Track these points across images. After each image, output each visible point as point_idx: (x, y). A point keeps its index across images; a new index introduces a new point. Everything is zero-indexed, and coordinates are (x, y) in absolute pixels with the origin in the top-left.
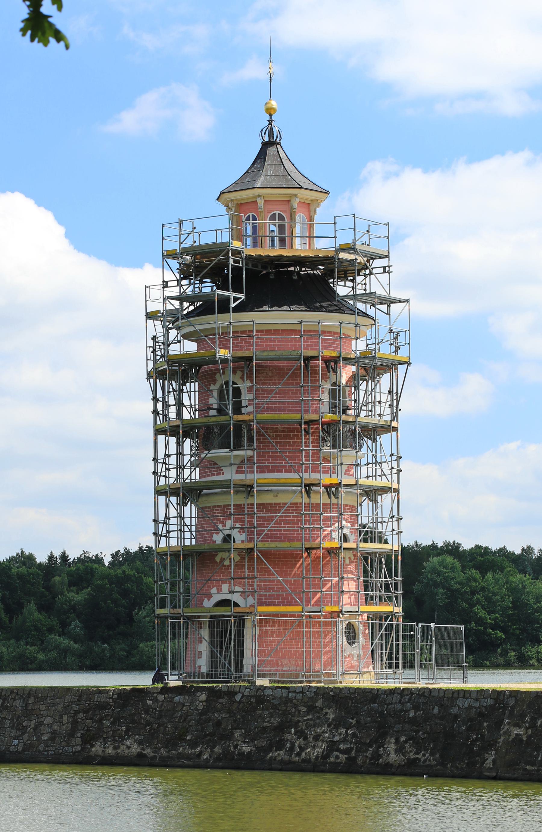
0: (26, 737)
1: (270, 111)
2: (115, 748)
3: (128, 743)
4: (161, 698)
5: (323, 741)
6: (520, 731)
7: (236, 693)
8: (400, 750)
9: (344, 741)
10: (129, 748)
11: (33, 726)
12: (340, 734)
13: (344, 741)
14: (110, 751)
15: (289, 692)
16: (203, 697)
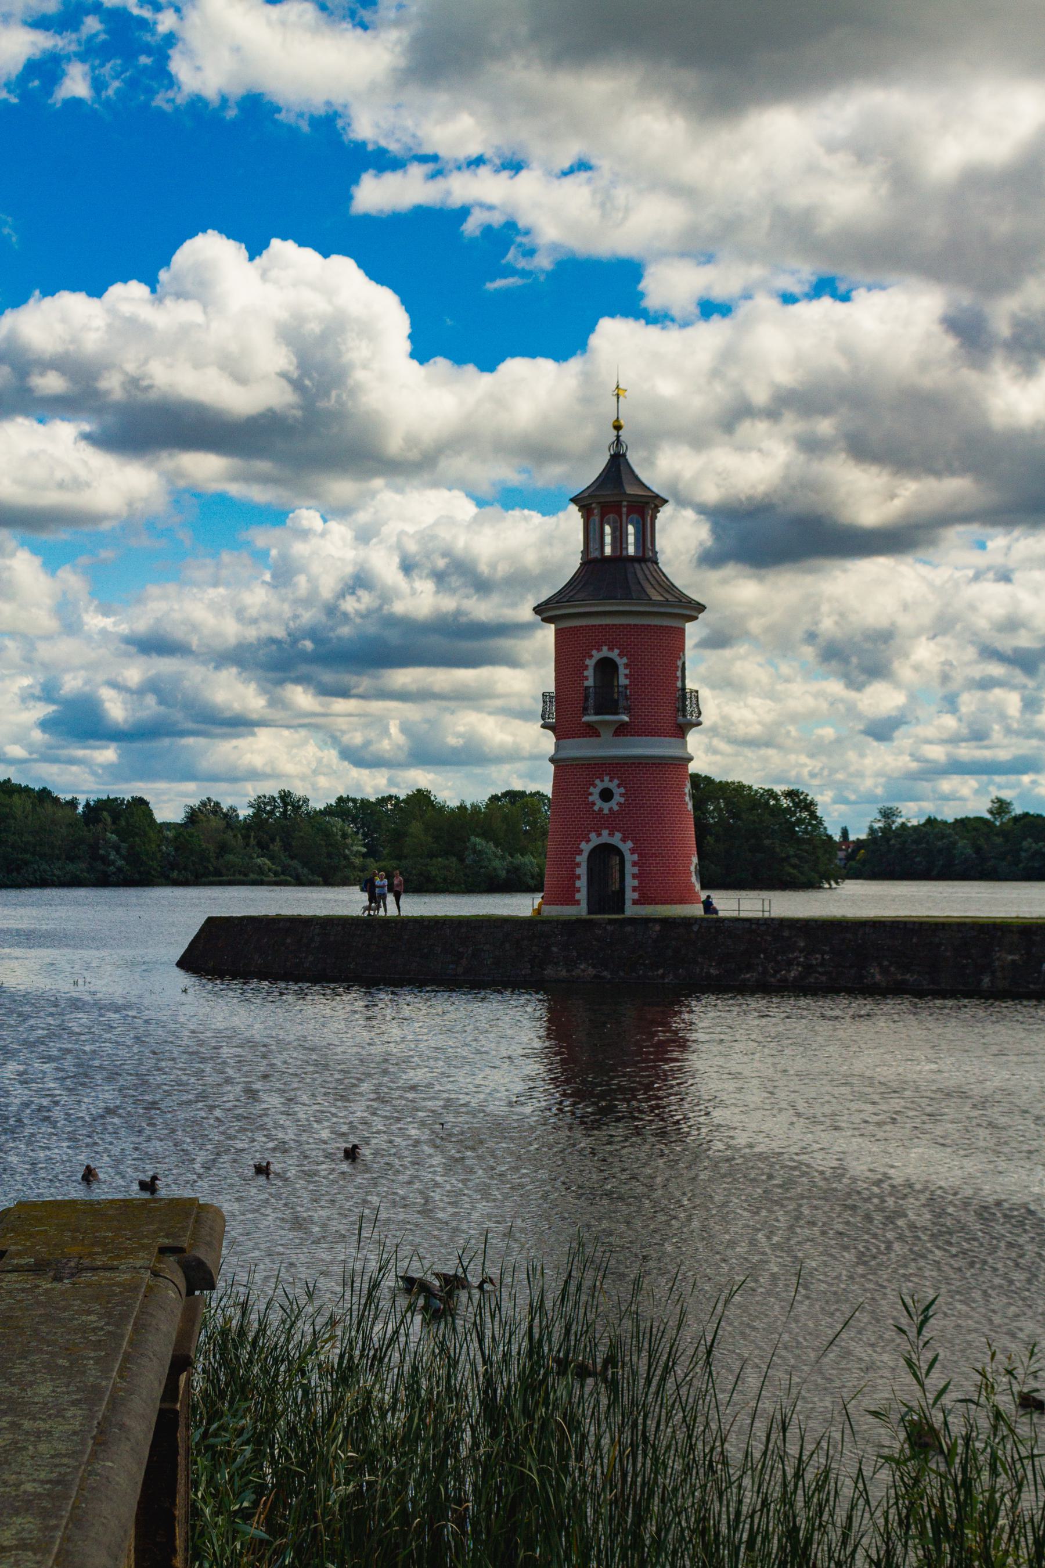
0: (464, 962)
1: (618, 427)
2: (568, 971)
3: (582, 967)
4: (609, 927)
5: (798, 964)
6: (1016, 957)
7: (692, 924)
8: (884, 971)
9: (822, 964)
10: (583, 971)
11: (470, 952)
12: (817, 959)
13: (822, 964)
14: (564, 973)
15: (751, 924)
16: (657, 928)
